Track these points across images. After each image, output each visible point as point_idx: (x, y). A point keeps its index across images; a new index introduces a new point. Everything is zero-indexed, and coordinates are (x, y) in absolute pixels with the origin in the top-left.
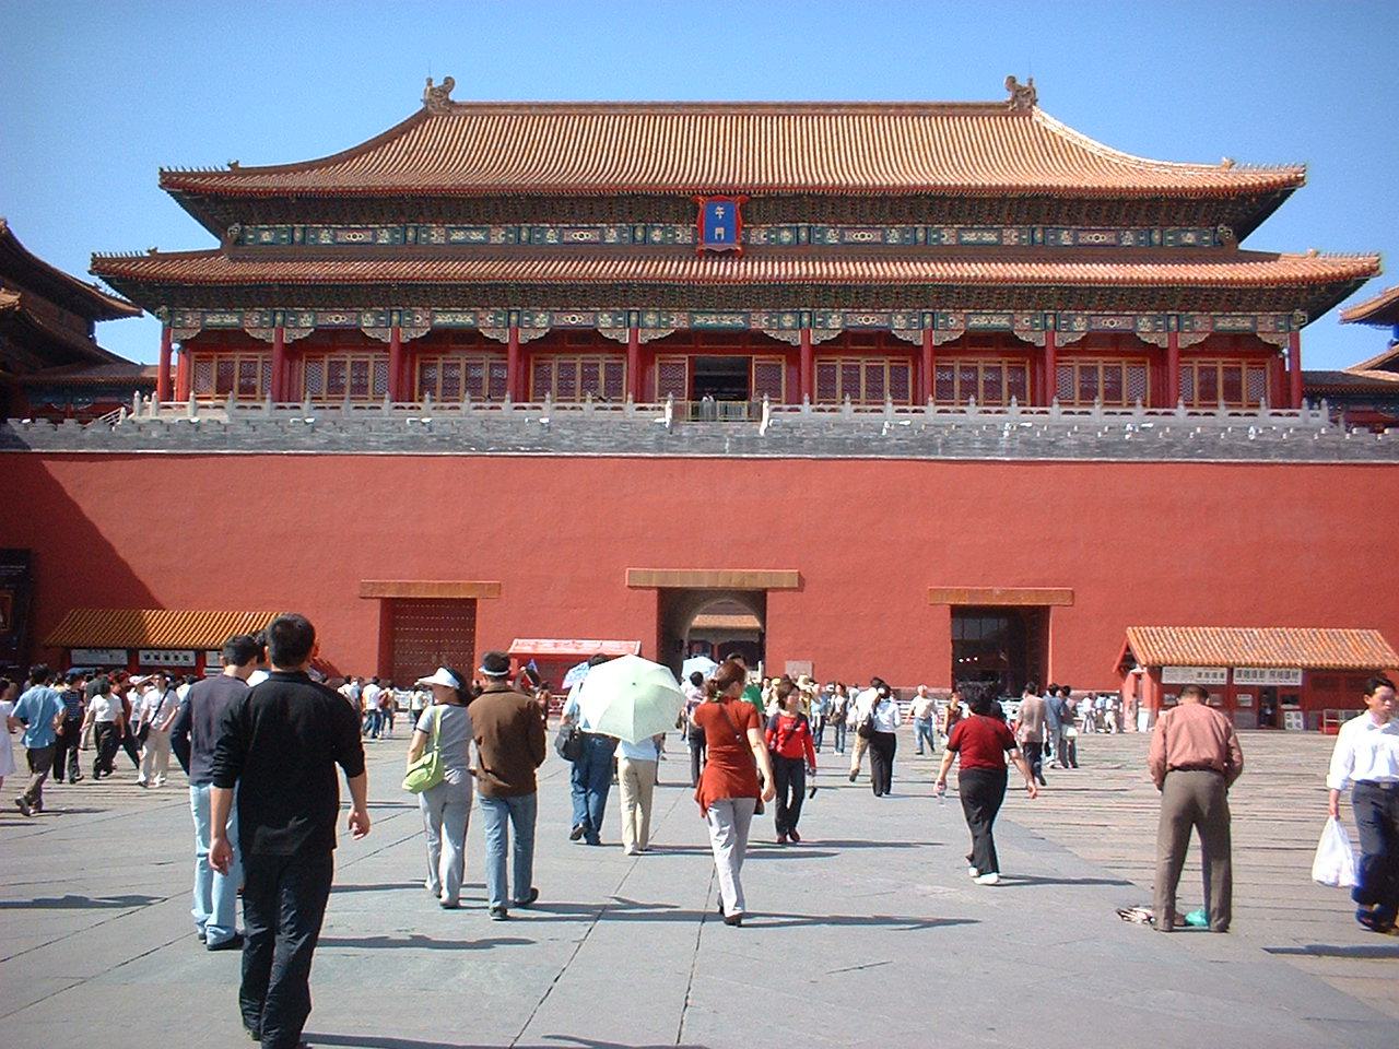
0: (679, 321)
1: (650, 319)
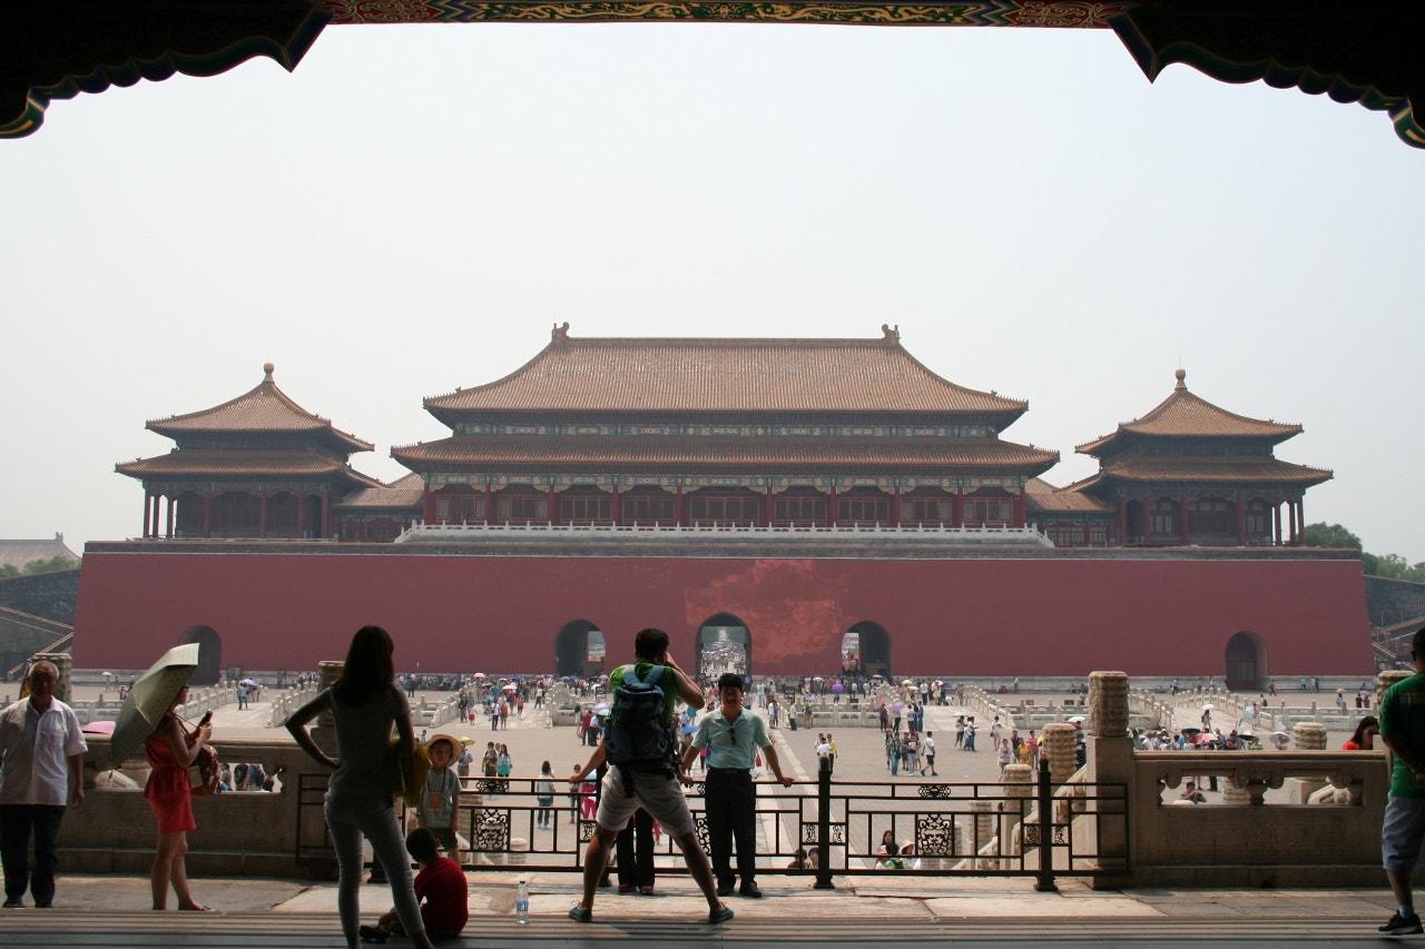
0: (703, 482)
1: (688, 481)
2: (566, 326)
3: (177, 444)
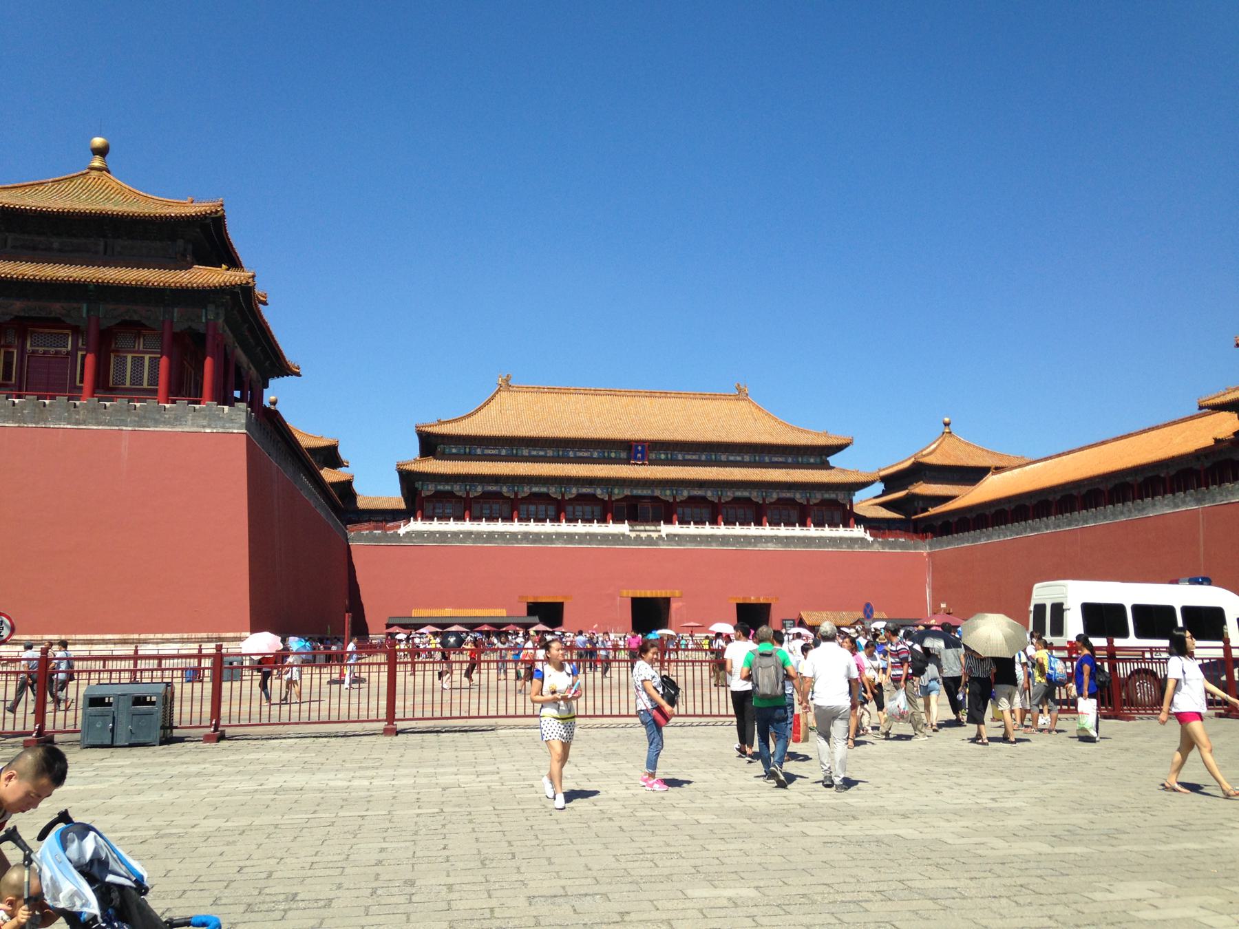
0: (627, 492)
1: (616, 491)
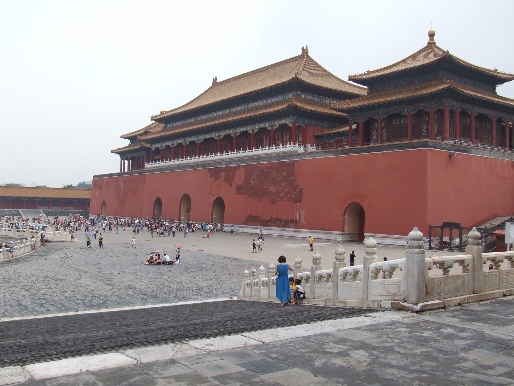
0: (203, 138)
2: (216, 78)
3: (131, 142)
